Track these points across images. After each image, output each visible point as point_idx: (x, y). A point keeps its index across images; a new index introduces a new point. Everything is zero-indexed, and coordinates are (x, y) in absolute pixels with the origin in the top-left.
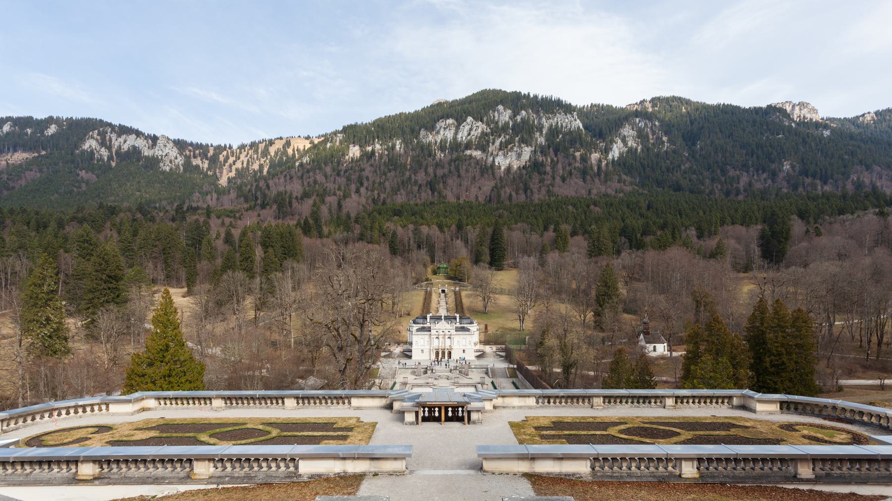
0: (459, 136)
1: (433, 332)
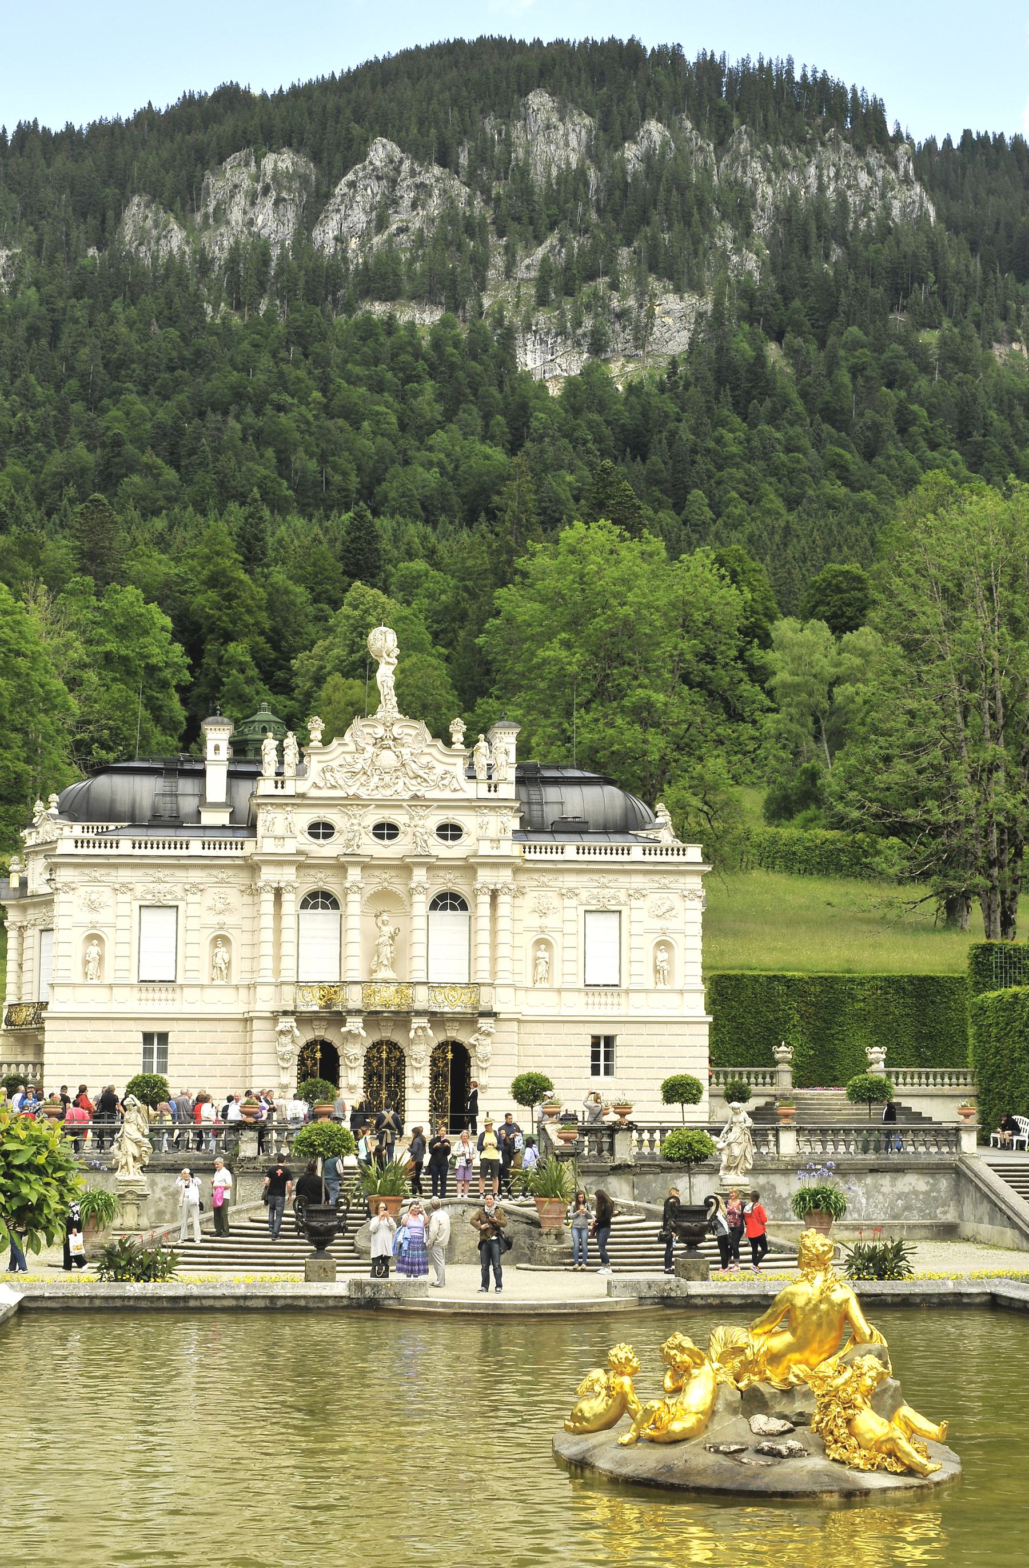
1: (282, 831)
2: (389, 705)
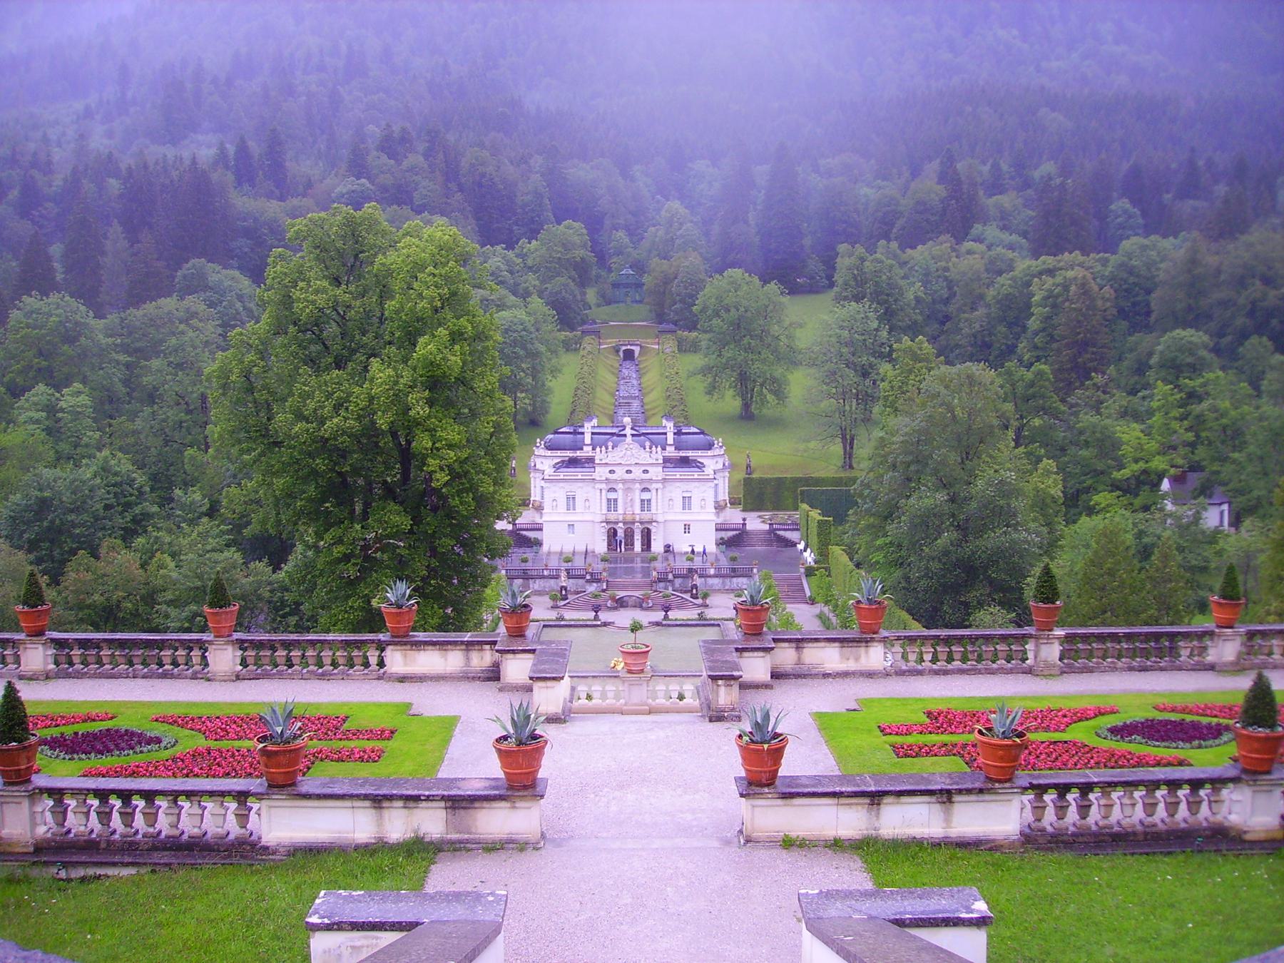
2: (629, 439)
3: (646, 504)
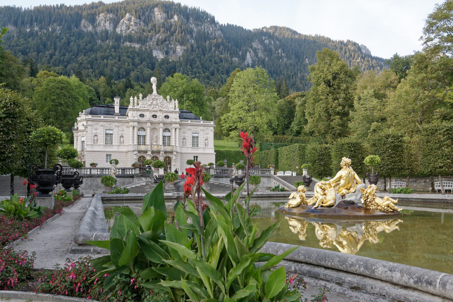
0: (118, 30)
2: (155, 92)
3: (166, 140)
